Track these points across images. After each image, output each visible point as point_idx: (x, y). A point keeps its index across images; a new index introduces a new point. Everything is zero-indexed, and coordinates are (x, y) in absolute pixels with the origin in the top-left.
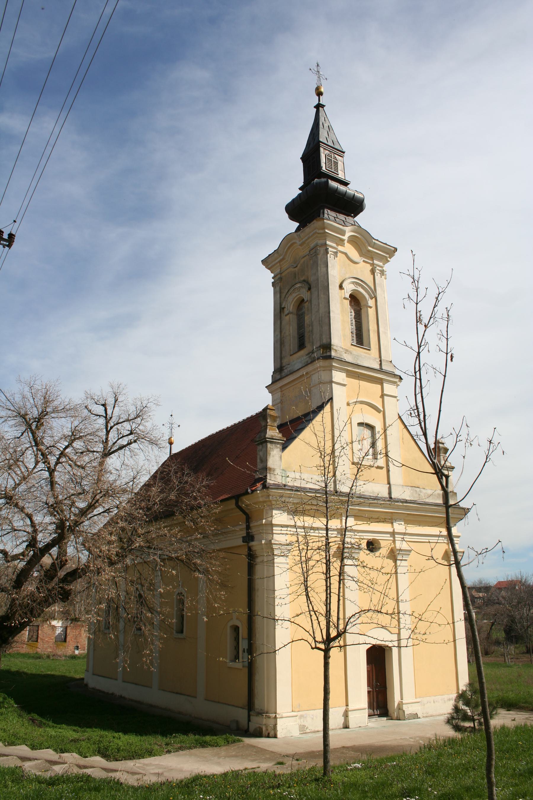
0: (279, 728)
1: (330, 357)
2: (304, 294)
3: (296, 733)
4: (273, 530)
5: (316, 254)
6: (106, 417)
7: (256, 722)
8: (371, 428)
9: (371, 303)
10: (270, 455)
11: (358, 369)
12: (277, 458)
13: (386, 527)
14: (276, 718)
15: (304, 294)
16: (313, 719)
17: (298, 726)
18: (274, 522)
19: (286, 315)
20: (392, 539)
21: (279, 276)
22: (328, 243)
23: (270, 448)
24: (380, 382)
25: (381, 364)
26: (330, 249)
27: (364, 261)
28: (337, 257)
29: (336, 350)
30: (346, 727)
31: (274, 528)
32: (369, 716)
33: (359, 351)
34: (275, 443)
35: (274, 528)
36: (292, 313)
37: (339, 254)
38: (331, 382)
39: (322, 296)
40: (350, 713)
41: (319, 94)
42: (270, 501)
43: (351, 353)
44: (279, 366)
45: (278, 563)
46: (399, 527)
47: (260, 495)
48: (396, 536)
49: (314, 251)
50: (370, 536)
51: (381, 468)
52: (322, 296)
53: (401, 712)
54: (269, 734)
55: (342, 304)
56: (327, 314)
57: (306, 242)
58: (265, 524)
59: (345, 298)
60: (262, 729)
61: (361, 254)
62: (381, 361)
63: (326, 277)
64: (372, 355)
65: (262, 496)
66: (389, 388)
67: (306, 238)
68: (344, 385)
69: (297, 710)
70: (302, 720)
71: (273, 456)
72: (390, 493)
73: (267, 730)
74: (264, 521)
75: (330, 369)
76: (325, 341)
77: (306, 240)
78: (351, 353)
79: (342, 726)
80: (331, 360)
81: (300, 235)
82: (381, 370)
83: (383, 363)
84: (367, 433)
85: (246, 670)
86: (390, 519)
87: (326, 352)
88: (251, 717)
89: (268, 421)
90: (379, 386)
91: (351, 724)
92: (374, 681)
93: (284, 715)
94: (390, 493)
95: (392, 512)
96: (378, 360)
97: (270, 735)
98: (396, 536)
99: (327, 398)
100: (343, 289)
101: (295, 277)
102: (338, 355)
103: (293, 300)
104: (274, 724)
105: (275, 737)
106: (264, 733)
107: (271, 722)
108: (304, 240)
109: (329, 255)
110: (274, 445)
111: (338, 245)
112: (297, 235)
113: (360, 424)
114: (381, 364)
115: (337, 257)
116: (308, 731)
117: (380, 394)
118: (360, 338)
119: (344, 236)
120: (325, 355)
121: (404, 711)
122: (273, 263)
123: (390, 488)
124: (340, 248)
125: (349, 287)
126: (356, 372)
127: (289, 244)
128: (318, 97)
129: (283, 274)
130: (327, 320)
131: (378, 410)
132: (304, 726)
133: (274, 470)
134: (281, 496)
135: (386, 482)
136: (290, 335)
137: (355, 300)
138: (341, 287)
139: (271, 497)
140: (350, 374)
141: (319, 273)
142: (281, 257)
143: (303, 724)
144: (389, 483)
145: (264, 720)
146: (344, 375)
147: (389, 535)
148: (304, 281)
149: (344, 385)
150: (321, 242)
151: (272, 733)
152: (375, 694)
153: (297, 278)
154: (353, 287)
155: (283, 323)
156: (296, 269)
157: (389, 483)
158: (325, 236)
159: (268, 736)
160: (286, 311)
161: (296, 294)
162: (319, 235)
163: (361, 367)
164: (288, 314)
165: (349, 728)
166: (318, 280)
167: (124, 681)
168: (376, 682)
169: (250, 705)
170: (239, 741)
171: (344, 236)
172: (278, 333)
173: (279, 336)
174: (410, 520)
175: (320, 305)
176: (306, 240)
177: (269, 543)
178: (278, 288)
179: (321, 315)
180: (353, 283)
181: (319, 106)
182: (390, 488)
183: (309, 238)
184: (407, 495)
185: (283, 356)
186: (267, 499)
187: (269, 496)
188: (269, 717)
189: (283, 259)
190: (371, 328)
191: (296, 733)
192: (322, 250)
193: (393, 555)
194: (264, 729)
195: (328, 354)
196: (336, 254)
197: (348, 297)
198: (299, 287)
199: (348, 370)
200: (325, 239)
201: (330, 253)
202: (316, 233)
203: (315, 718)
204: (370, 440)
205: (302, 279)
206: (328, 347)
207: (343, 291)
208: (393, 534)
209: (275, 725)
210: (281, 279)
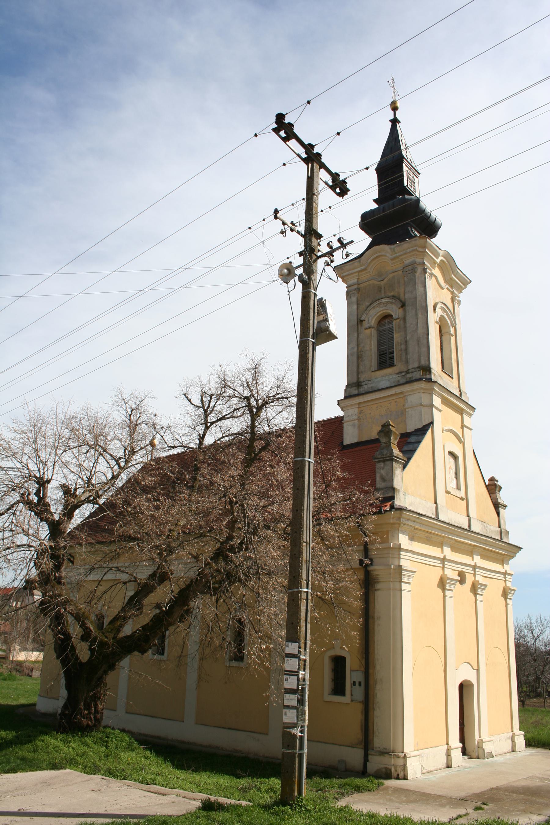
1: (429, 380)
2: (395, 311)
4: (400, 555)
5: (414, 271)
7: (376, 763)
9: (452, 331)
11: (451, 396)
15: (395, 311)
19: (366, 329)
21: (356, 287)
27: (447, 288)
30: (449, 766)
36: (373, 327)
41: (395, 108)
46: (478, 560)
47: (392, 516)
49: (410, 268)
53: (480, 750)
54: (398, 775)
56: (426, 336)
57: (401, 258)
60: (390, 770)
61: (446, 281)
63: (424, 297)
67: (402, 253)
72: (470, 526)
73: (396, 771)
75: (430, 392)
76: (423, 363)
77: (402, 255)
79: (445, 766)
81: (394, 249)
85: (360, 707)
87: (426, 375)
88: (370, 757)
89: (392, 438)
97: (400, 776)
101: (380, 291)
103: (376, 315)
105: (405, 778)
107: (400, 762)
108: (398, 254)
112: (390, 249)
119: (437, 259)
121: (484, 750)
122: (350, 272)
127: (375, 256)
128: (393, 112)
129: (362, 286)
130: (425, 342)
136: (371, 350)
142: (363, 268)
145: (393, 760)
148: (394, 297)
150: (418, 260)
151: (401, 775)
153: (383, 292)
156: (382, 283)
157: (468, 516)
159: (398, 778)
160: (365, 324)
161: (381, 309)
162: (418, 253)
163: (452, 395)
164: (369, 328)
165: (451, 767)
166: (416, 298)
167: (127, 713)
171: (437, 259)
173: (356, 349)
176: (402, 255)
178: (354, 299)
181: (395, 122)
183: (405, 254)
185: (360, 370)
188: (399, 757)
189: (365, 269)
191: (419, 775)
192: (419, 269)
194: (393, 770)
195: (428, 376)
198: (387, 302)
200: (423, 258)
202: (416, 250)
205: (392, 294)
209: (405, 765)
210: (358, 290)
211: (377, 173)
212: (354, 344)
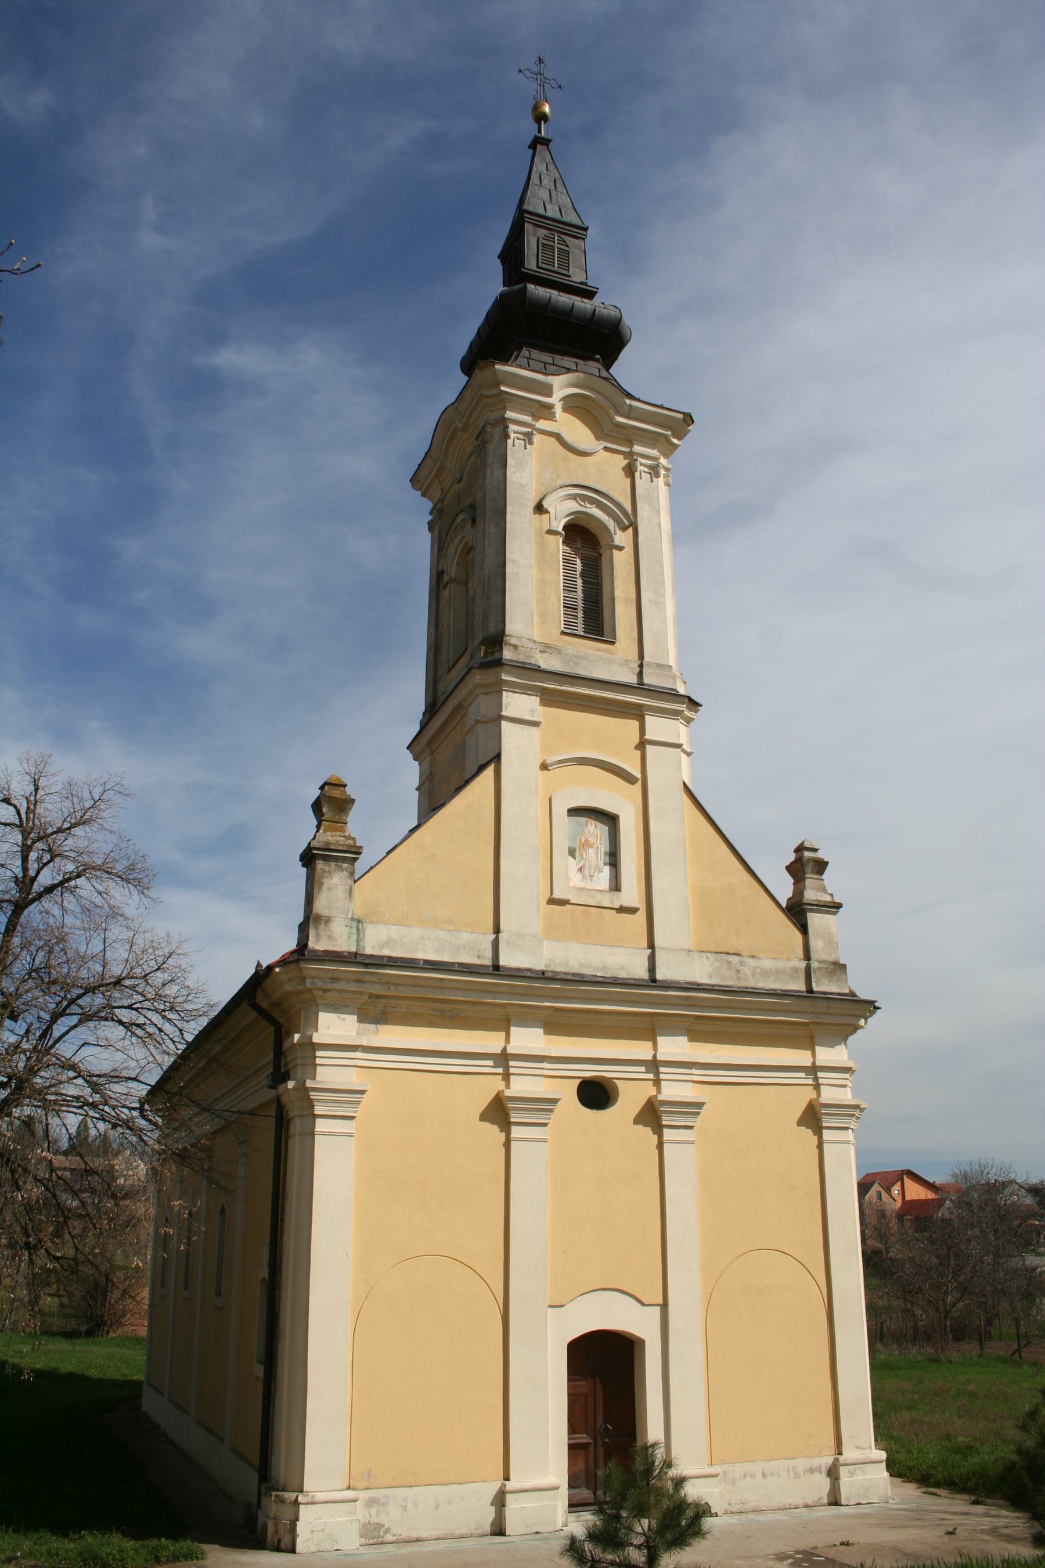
0: (301, 1527)
1: (499, 663)
3: (350, 1542)
4: (315, 1057)
6: (21, 825)
8: (610, 820)
9: (622, 538)
10: (320, 888)
11: (572, 685)
12: (340, 893)
13: (641, 1050)
14: (296, 1503)
16: (405, 1508)
17: (356, 1526)
18: (316, 1038)
20: (651, 1076)
22: (509, 414)
23: (324, 871)
24: (638, 713)
25: (640, 674)
26: (512, 427)
27: (606, 449)
28: (531, 443)
29: (515, 647)
30: (498, 1530)
31: (318, 1053)
32: (570, 1506)
33: (589, 648)
34: (337, 859)
35: (318, 1053)
37: (537, 438)
38: (500, 718)
39: (492, 530)
40: (509, 1498)
42: (310, 991)
43: (559, 651)
44: (430, 700)
45: (324, 1134)
46: (673, 1047)
47: (283, 978)
48: (662, 1069)
50: (589, 1072)
51: (633, 911)
52: (492, 530)
55: (541, 546)
58: (300, 1044)
59: (550, 532)
61: (600, 433)
62: (641, 666)
64: (620, 655)
65: (290, 980)
66: (657, 727)
68: (535, 724)
69: (365, 1484)
70: (373, 1511)
71: (330, 889)
72: (652, 969)
73: (277, 1531)
74: (297, 1036)
75: (497, 689)
76: (492, 629)
77: (470, 417)
78: (559, 651)
79: (488, 1529)
80: (499, 669)
82: (640, 687)
83: (646, 671)
84: (596, 832)
86: (648, 1029)
87: (493, 653)
89: (324, 810)
90: (635, 724)
91: (511, 1525)
92: (600, 1419)
93: (320, 1497)
94: (652, 969)
95: (651, 1014)
96: (635, 666)
97: (283, 1545)
98: (662, 1069)
99: (491, 755)
100: (547, 512)
102: (521, 658)
103: (455, 553)
104: (293, 1517)
105: (293, 1550)
106: (269, 1539)
107: (286, 1512)
109: (510, 442)
110: (333, 864)
111: (536, 417)
113: (574, 812)
114: (640, 674)
115: (531, 443)
116: (389, 1538)
117: (637, 740)
118: (593, 617)
119: (550, 396)
120: (490, 658)
123: (652, 959)
124: (542, 424)
125: (562, 509)
126: (565, 692)
131: (630, 779)
132: (379, 1526)
133: (328, 920)
134: (335, 979)
135: (645, 943)
137: (582, 536)
138: (539, 509)
139: (308, 982)
140: (549, 698)
141: (488, 481)
143: (375, 1519)
144: (651, 946)
146: (534, 701)
147: (643, 1069)
149: (535, 724)
150: (493, 416)
151: (286, 1541)
152: (601, 1450)
154: (573, 506)
155: (441, 606)
157: (651, 946)
158: (504, 401)
159: (278, 1548)
160: (446, 578)
163: (580, 681)
165: (505, 1535)
168: (605, 1422)
170: (190, 1556)
171: (550, 396)
172: (433, 629)
174: (700, 1031)
175: (487, 552)
176: (470, 417)
177: (304, 1091)
179: (486, 572)
180: (574, 497)
182: (652, 959)
183: (472, 412)
184: (700, 971)
186: (301, 987)
187: (303, 979)
188: (282, 1501)
189: (441, 468)
190: (618, 593)
191: (350, 1542)
192: (497, 432)
193: (651, 1115)
195: (496, 656)
196: (528, 438)
197: (560, 529)
199: (544, 688)
201: (512, 435)
202: (482, 396)
203: (410, 1506)
204: (604, 847)
206: (497, 640)
207: (545, 517)
208: (654, 1065)
211: (503, 263)
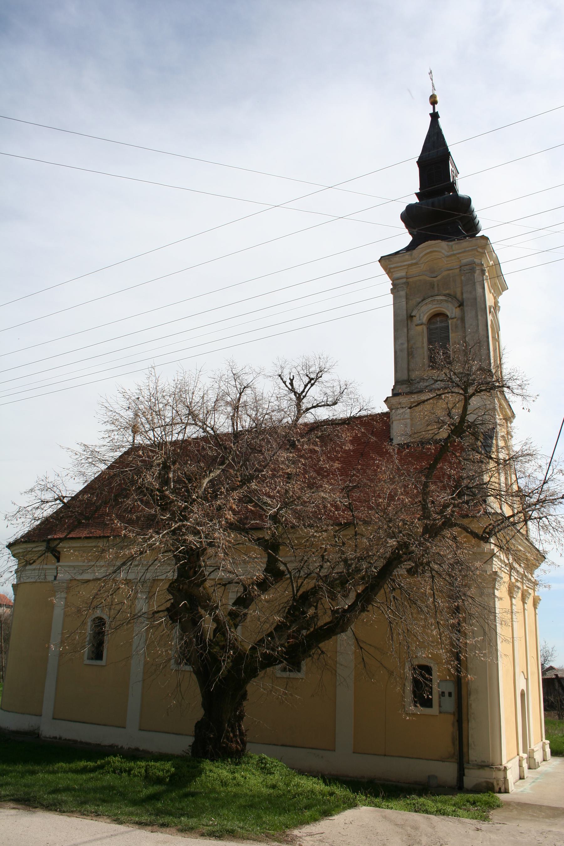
2: (451, 310)
5: (473, 271)
7: (472, 777)
15: (451, 310)
19: (416, 325)
21: (404, 280)
36: (425, 324)
49: (467, 267)
53: (532, 760)
54: (500, 789)
56: (485, 339)
57: (458, 256)
60: (492, 784)
63: (483, 299)
67: (460, 251)
73: (498, 784)
79: (518, 777)
81: (452, 247)
85: (450, 719)
88: (466, 771)
101: (433, 288)
105: (506, 791)
107: (501, 775)
108: (455, 252)
112: (448, 245)
121: (535, 759)
122: (399, 264)
127: (428, 251)
128: (432, 106)
129: (411, 280)
130: (486, 344)
136: (423, 347)
142: (414, 261)
145: (494, 773)
148: (449, 295)
153: (436, 289)
156: (435, 279)
159: (500, 792)
160: (416, 320)
161: (435, 306)
162: (477, 254)
164: (421, 324)
165: (524, 779)
166: (475, 299)
167: (140, 730)
169: (461, 757)
173: (405, 346)
178: (403, 293)
181: (435, 116)
185: (410, 368)
188: (499, 770)
189: (416, 264)
194: (495, 784)
198: (442, 300)
200: (481, 259)
205: (447, 292)
209: (505, 778)
210: (407, 283)
211: (419, 166)
212: (403, 340)
